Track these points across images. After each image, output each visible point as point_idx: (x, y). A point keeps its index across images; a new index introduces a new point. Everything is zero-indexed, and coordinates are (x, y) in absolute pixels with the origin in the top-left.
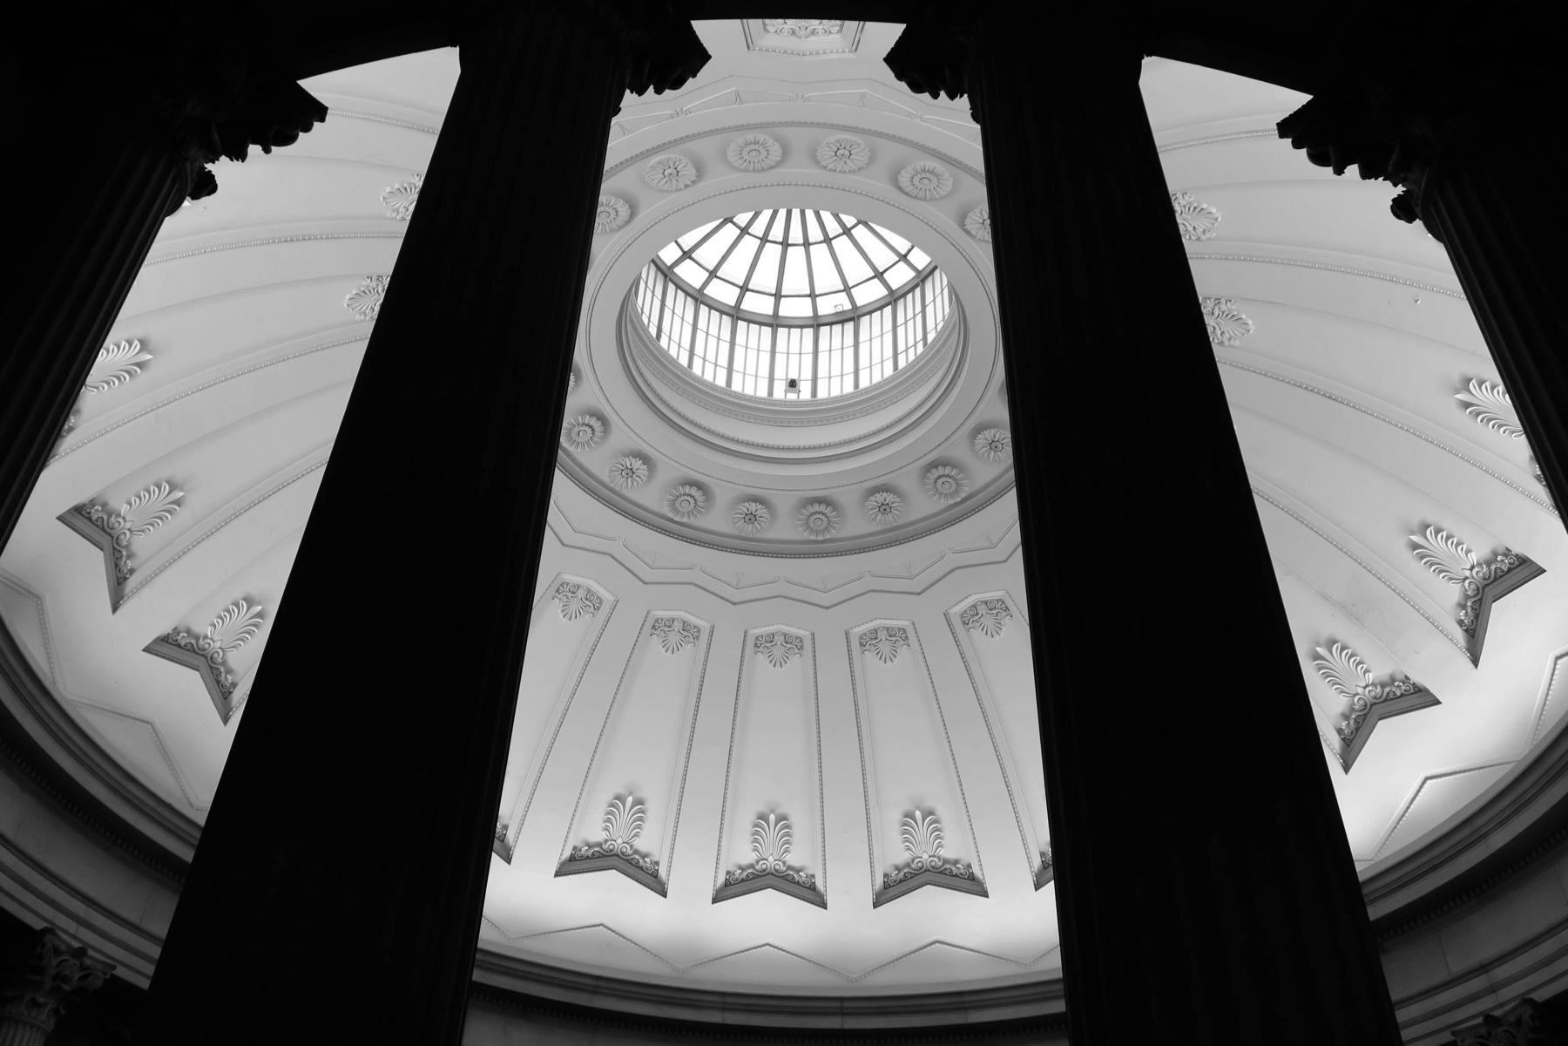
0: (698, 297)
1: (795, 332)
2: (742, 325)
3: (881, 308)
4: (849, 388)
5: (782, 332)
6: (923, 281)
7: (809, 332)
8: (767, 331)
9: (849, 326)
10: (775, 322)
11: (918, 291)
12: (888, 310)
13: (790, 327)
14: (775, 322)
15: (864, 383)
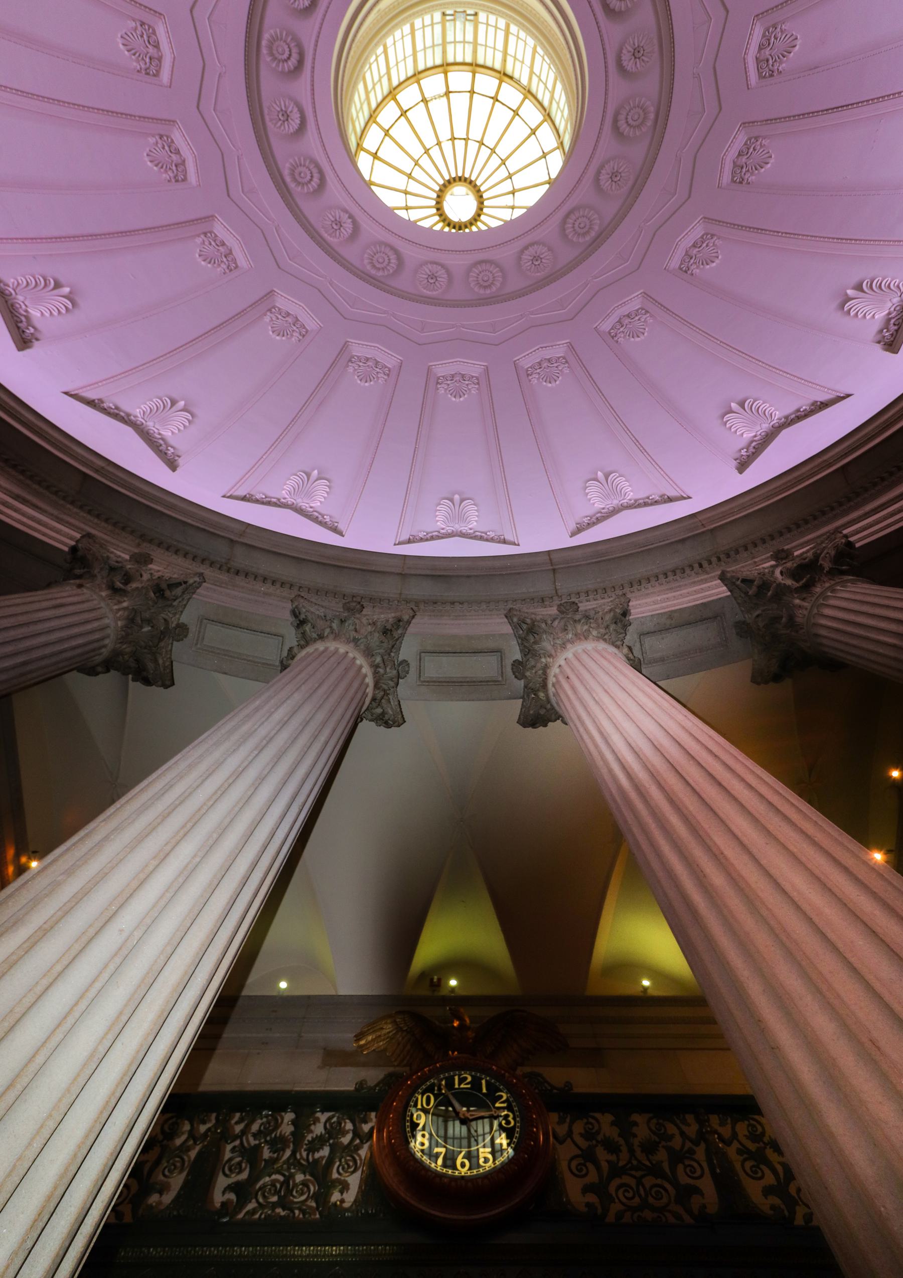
0: (528, 93)
1: (459, 59)
2: (498, 66)
3: (400, 84)
4: (418, 23)
5: (469, 59)
6: (371, 116)
7: (450, 59)
8: (480, 61)
9: (421, 67)
10: (474, 67)
11: (374, 105)
12: (395, 83)
13: (464, 64)
14: (474, 67)
15: (407, 28)
